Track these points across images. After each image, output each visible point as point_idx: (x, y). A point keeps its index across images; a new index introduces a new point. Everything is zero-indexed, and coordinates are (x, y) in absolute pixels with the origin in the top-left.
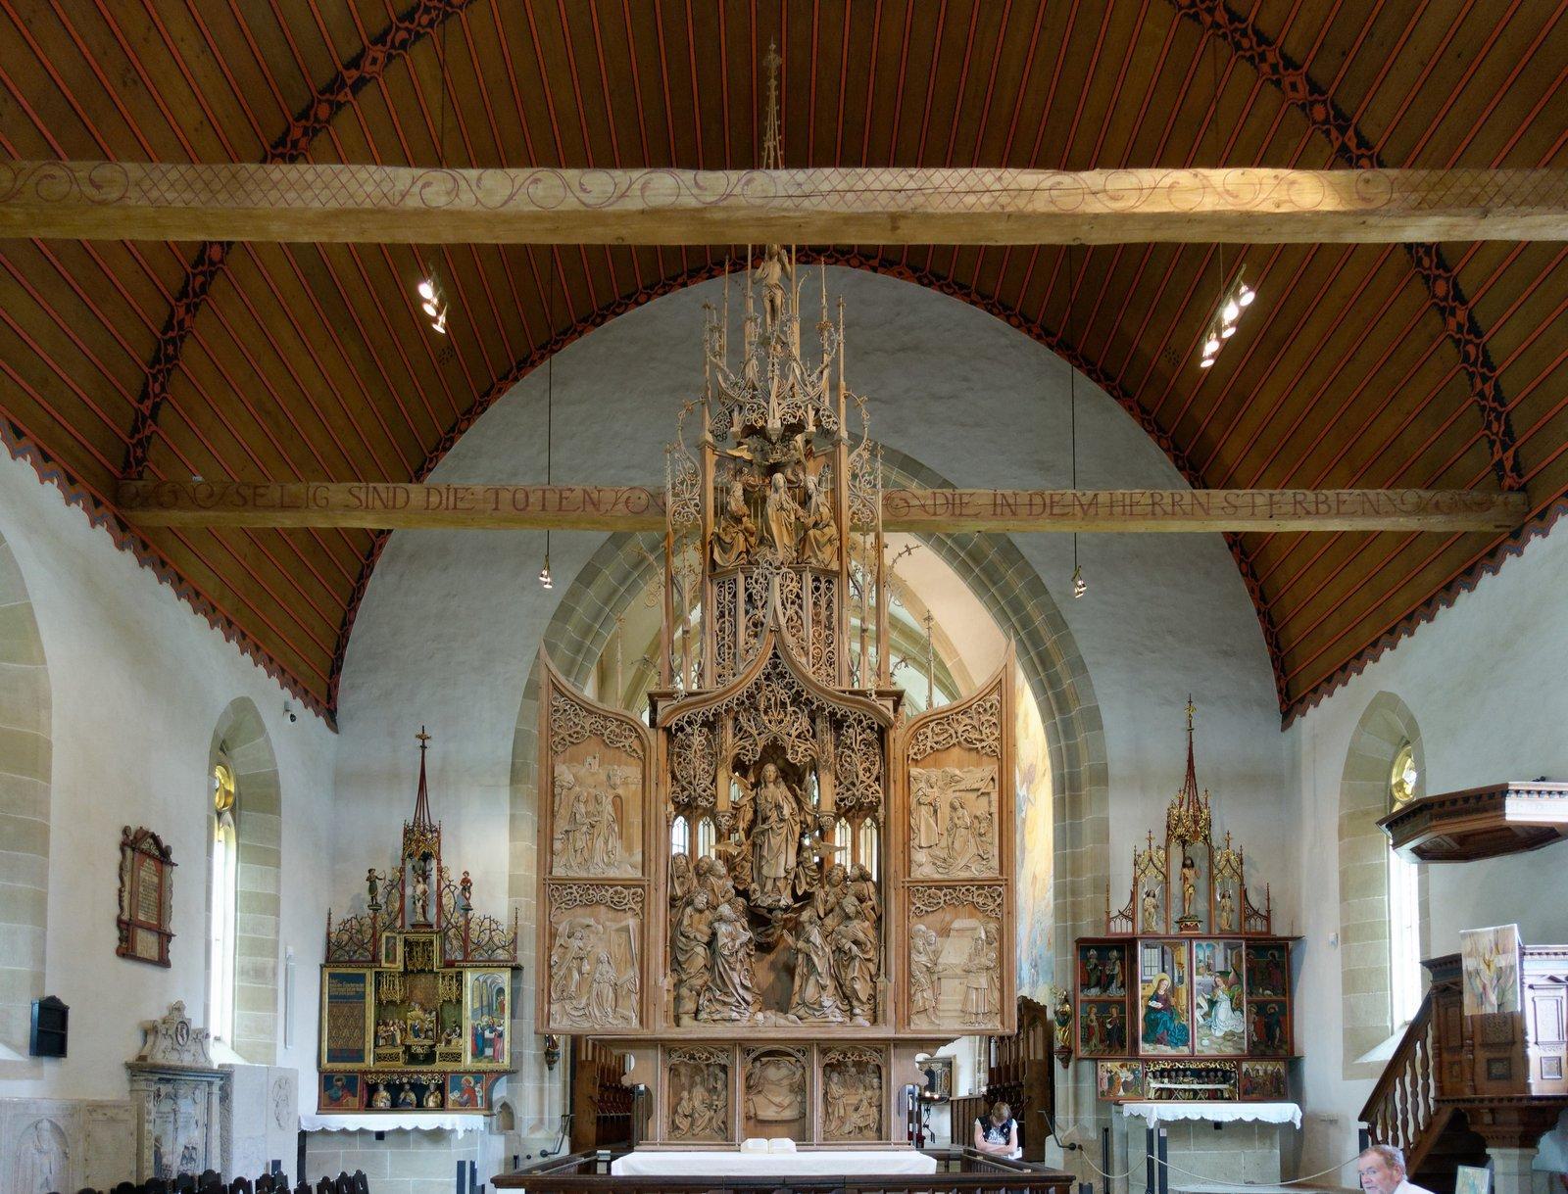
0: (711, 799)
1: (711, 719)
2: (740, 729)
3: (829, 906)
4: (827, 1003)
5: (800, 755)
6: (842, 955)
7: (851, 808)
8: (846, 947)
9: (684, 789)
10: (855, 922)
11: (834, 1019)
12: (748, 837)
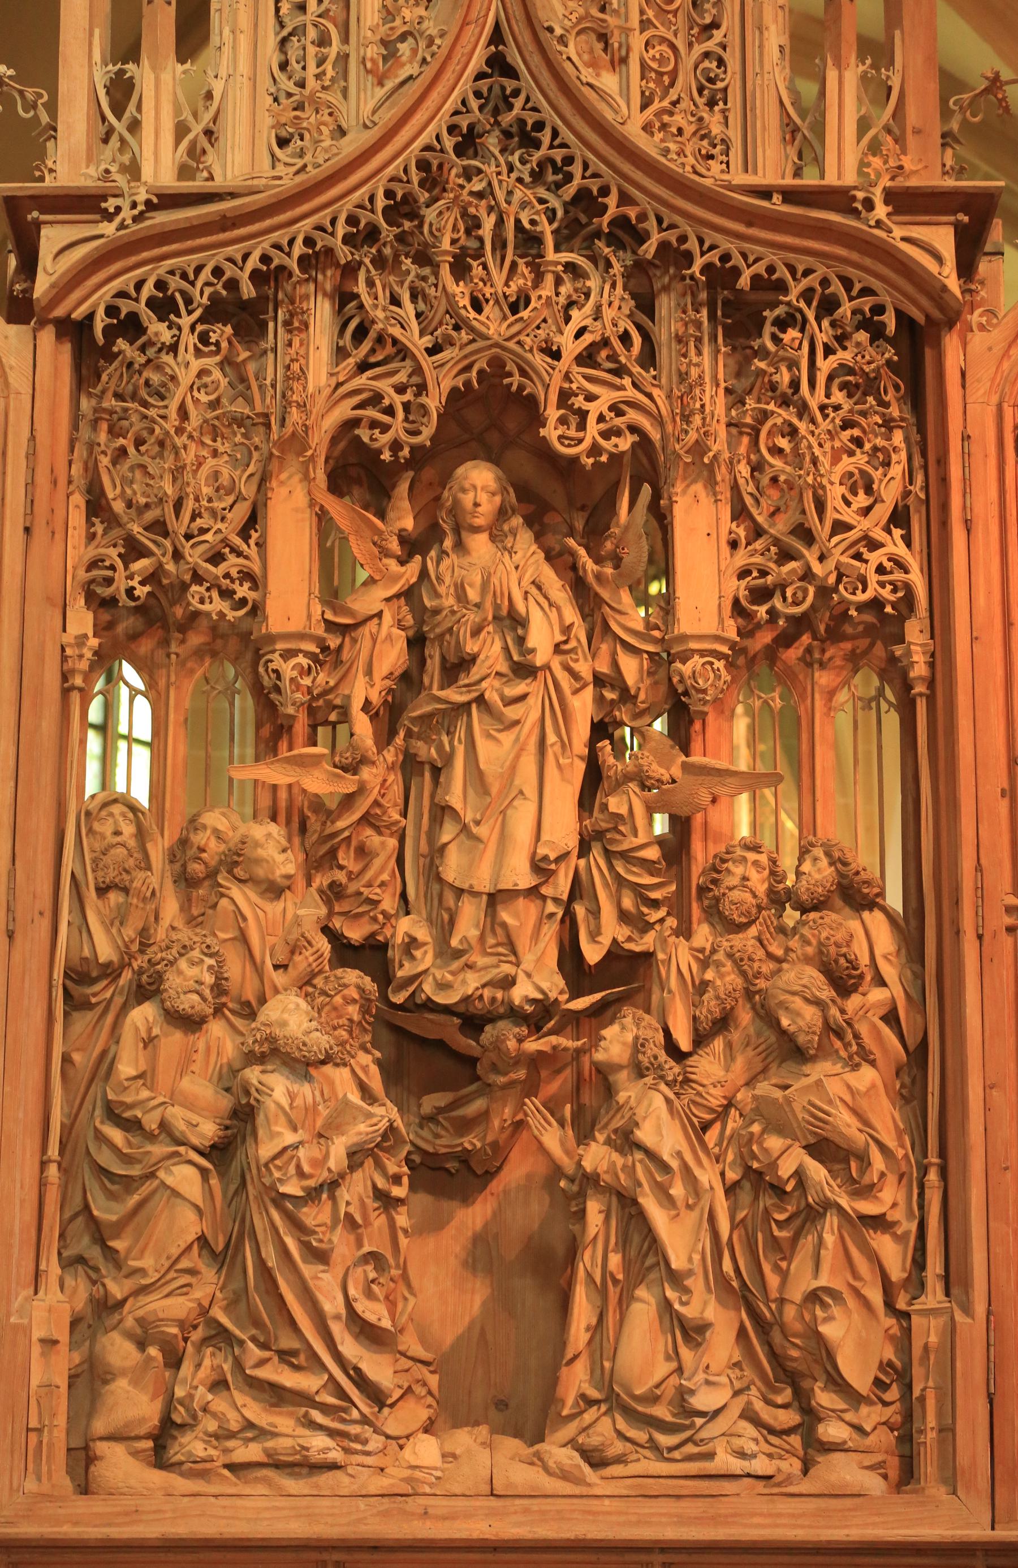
0: (243, 591)
1: (248, 290)
2: (361, 333)
3: (710, 1006)
4: (704, 1400)
5: (593, 428)
6: (767, 1200)
7: (801, 623)
8: (786, 1169)
9: (134, 550)
10: (819, 1070)
11: (737, 1465)
12: (385, 736)
